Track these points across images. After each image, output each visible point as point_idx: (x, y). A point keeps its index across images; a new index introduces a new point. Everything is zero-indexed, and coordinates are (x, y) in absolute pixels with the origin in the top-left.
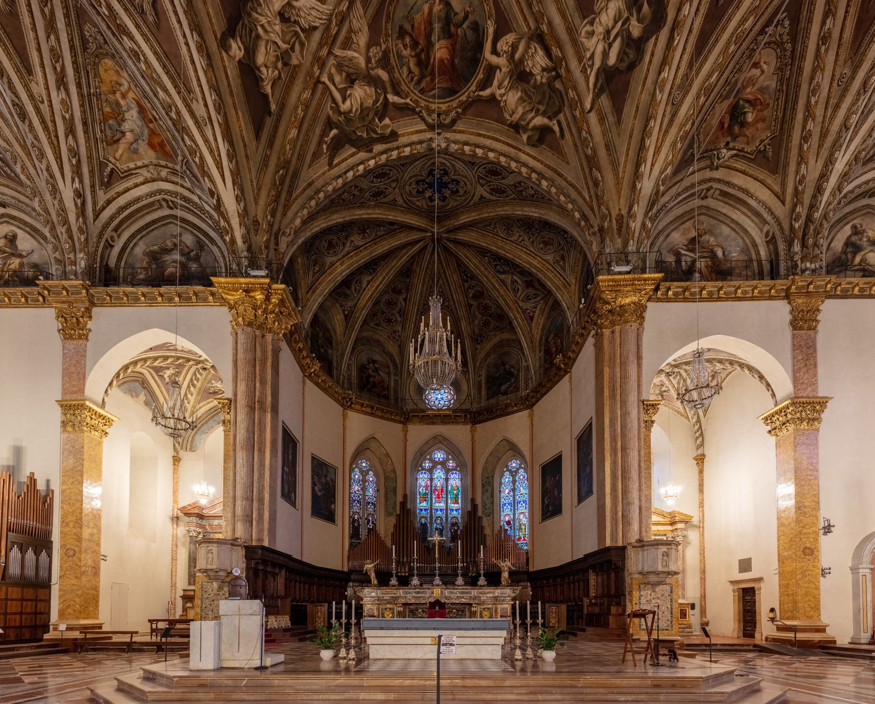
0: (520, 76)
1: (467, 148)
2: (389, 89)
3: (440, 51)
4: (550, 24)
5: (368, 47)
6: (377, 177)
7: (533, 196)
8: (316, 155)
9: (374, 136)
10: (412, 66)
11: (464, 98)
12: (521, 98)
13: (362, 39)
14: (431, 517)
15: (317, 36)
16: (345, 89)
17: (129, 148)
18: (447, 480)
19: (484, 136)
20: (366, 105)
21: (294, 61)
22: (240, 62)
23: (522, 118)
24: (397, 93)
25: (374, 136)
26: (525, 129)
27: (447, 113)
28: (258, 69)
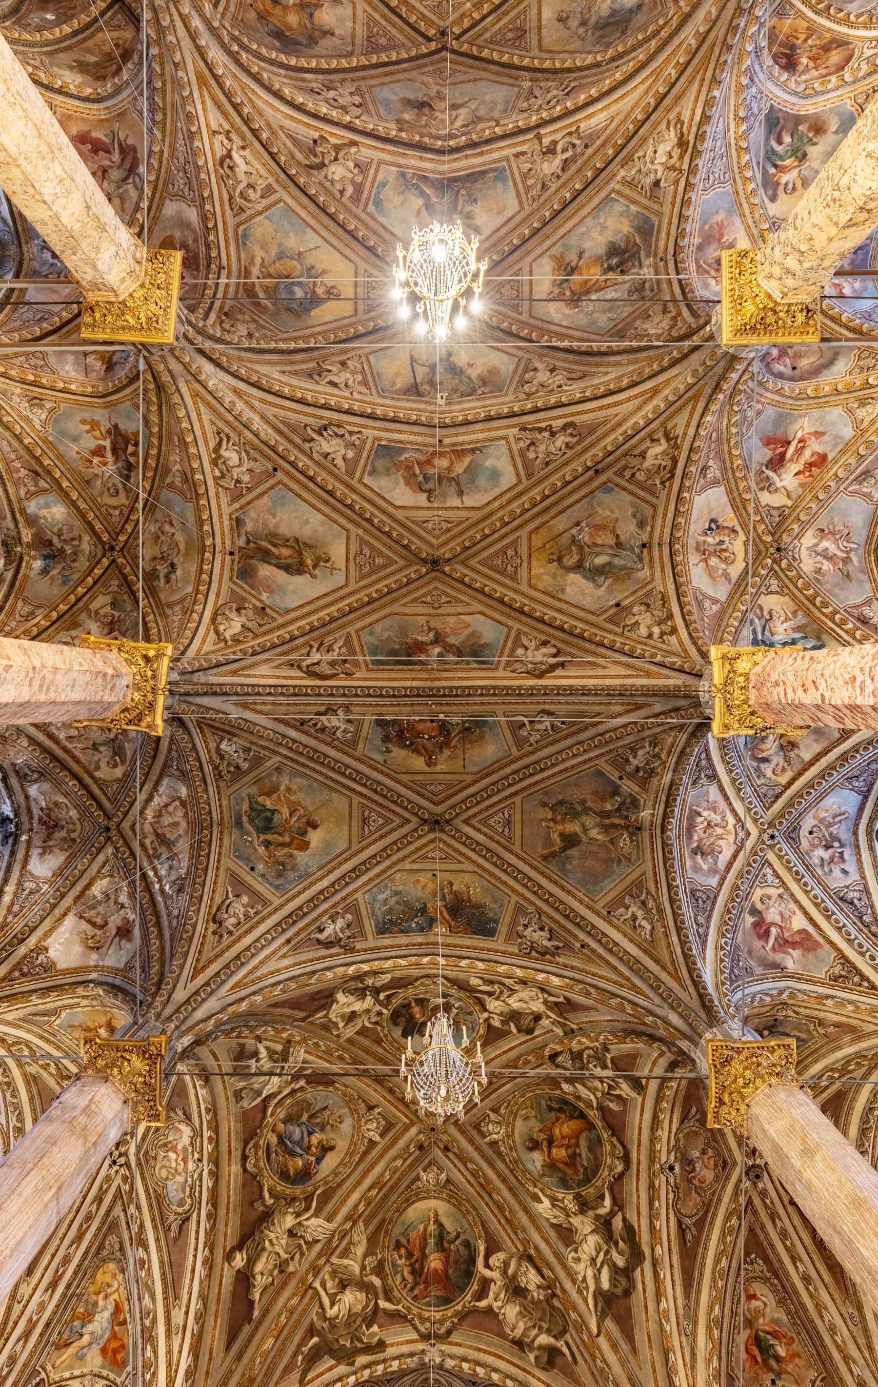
0: (517, 1291)
1: (465, 1366)
2: (381, 1295)
3: (434, 1262)
4: (537, 1249)
5: (365, 1256)
8: (287, 1370)
9: (359, 1345)
10: (406, 1274)
12: (520, 1313)
13: (360, 1250)
15: (318, 1247)
16: (336, 1294)
20: (354, 1311)
21: (291, 1269)
24: (389, 1299)
25: (359, 1345)
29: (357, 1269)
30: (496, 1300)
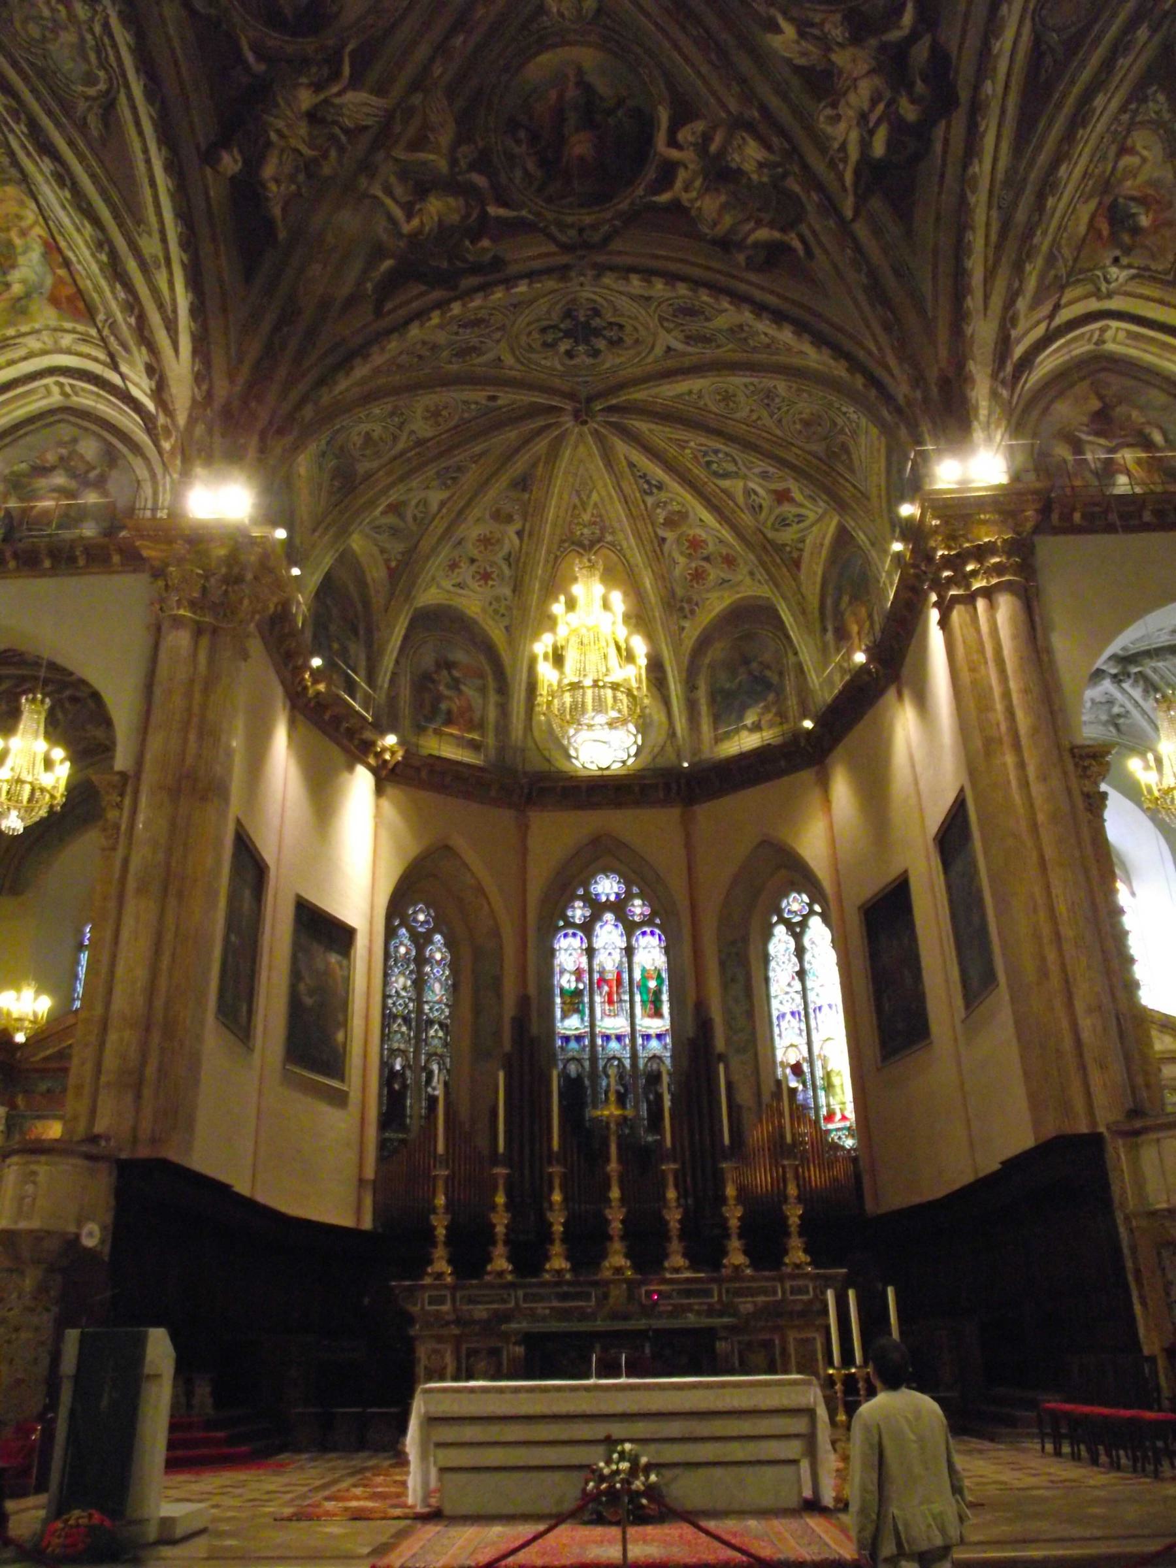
3: (580, 146)
6: (465, 326)
7: (768, 346)
11: (624, 206)
13: (445, 139)
14: (594, 1058)
17: (13, 307)
18: (629, 951)
19: (667, 258)
22: (233, 178)
23: (733, 230)
26: (740, 246)
27: (594, 227)
28: (263, 185)
29: (443, 165)
30: (686, 189)
